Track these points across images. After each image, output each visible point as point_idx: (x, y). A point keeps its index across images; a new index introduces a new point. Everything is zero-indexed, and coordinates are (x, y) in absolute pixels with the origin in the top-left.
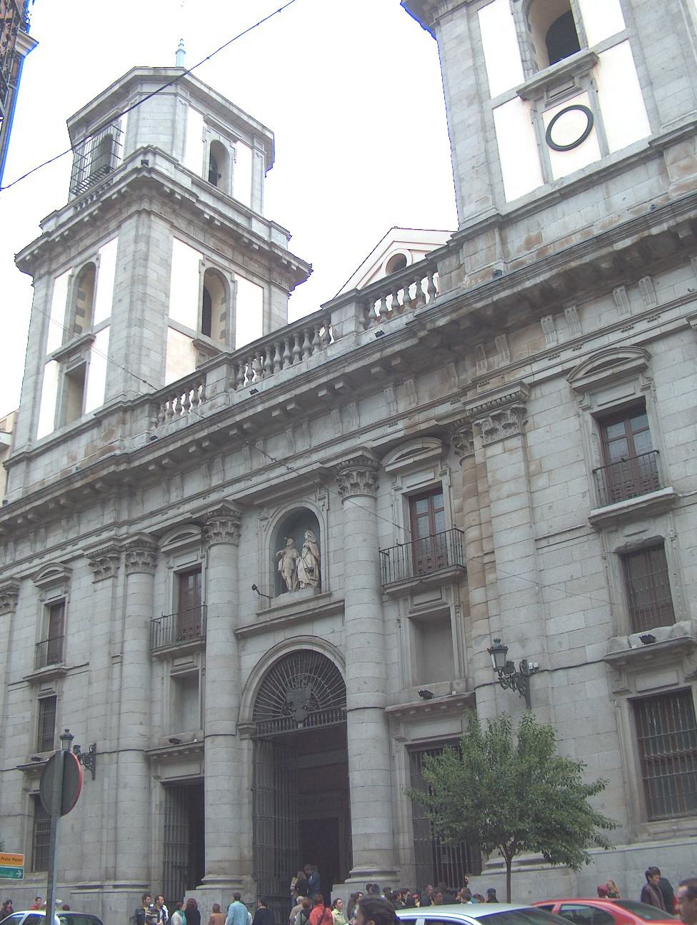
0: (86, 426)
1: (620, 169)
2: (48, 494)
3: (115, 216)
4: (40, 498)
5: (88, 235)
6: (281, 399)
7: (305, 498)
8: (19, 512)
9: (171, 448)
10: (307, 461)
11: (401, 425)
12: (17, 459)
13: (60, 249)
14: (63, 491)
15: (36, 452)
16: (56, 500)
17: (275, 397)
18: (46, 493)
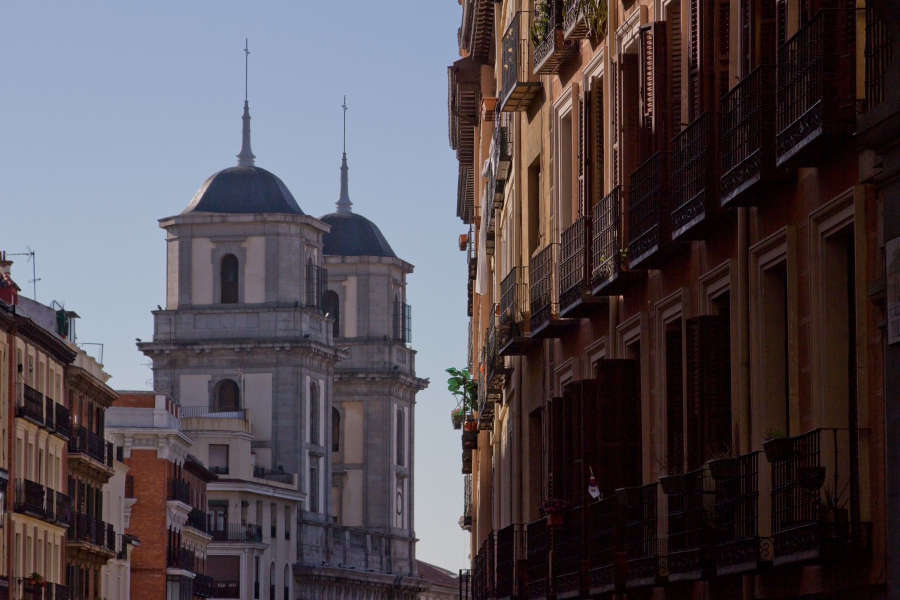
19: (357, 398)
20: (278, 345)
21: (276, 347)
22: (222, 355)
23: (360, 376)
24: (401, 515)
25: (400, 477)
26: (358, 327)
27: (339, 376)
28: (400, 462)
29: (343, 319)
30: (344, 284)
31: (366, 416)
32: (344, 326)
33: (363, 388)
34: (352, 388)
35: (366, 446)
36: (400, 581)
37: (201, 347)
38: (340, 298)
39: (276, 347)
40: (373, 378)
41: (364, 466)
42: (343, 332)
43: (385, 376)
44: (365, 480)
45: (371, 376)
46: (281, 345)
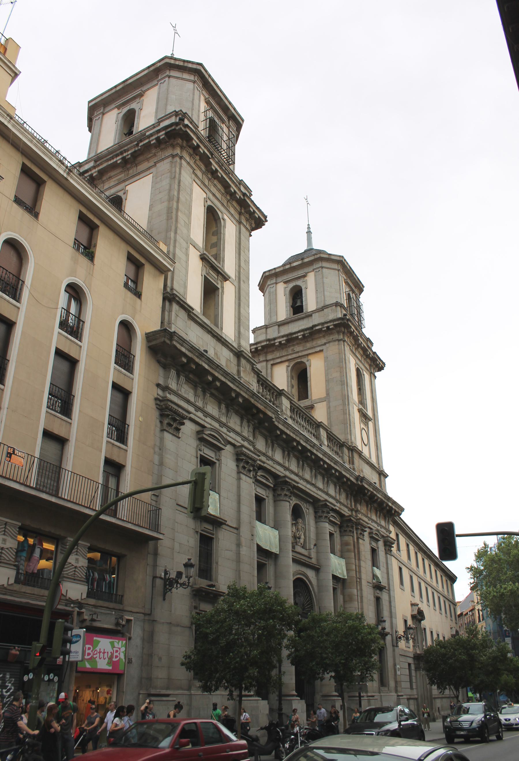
0: (231, 347)
1: (375, 469)
2: (237, 387)
3: (235, 208)
4: (232, 383)
5: (219, 190)
6: (327, 461)
7: (302, 503)
8: (217, 374)
9: (292, 434)
10: (316, 491)
11: (338, 505)
12: (186, 306)
13: (203, 167)
14: (247, 396)
15: (195, 317)
16: (238, 395)
17: (326, 457)
18: (237, 384)
19: (318, 349)
20: (154, 137)
21: (152, 140)
22: (110, 178)
23: (317, 328)
24: (367, 447)
25: (364, 417)
26: (317, 302)
27: (302, 333)
28: (362, 401)
29: (306, 300)
30: (306, 279)
31: (326, 359)
32: (307, 305)
33: (324, 341)
34: (314, 343)
35: (328, 381)
36: (361, 482)
37: (90, 173)
38: (303, 288)
39: (152, 140)
40: (328, 327)
41: (327, 399)
42: (307, 308)
43: (337, 322)
44: (329, 408)
45: (326, 325)
46: (156, 136)
